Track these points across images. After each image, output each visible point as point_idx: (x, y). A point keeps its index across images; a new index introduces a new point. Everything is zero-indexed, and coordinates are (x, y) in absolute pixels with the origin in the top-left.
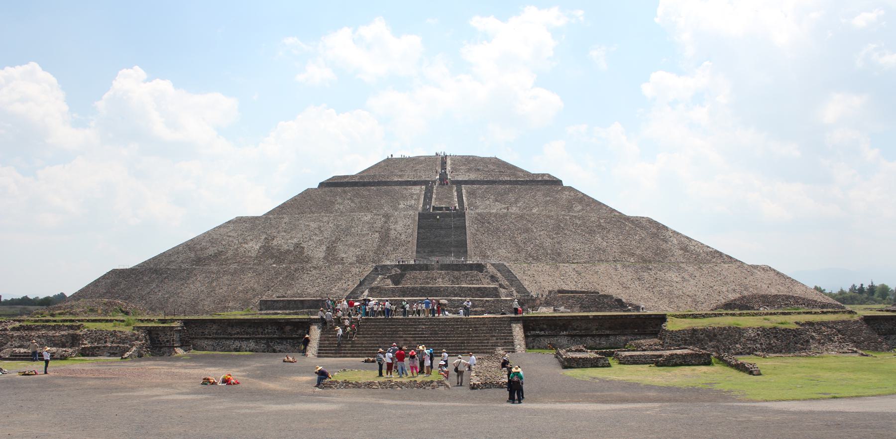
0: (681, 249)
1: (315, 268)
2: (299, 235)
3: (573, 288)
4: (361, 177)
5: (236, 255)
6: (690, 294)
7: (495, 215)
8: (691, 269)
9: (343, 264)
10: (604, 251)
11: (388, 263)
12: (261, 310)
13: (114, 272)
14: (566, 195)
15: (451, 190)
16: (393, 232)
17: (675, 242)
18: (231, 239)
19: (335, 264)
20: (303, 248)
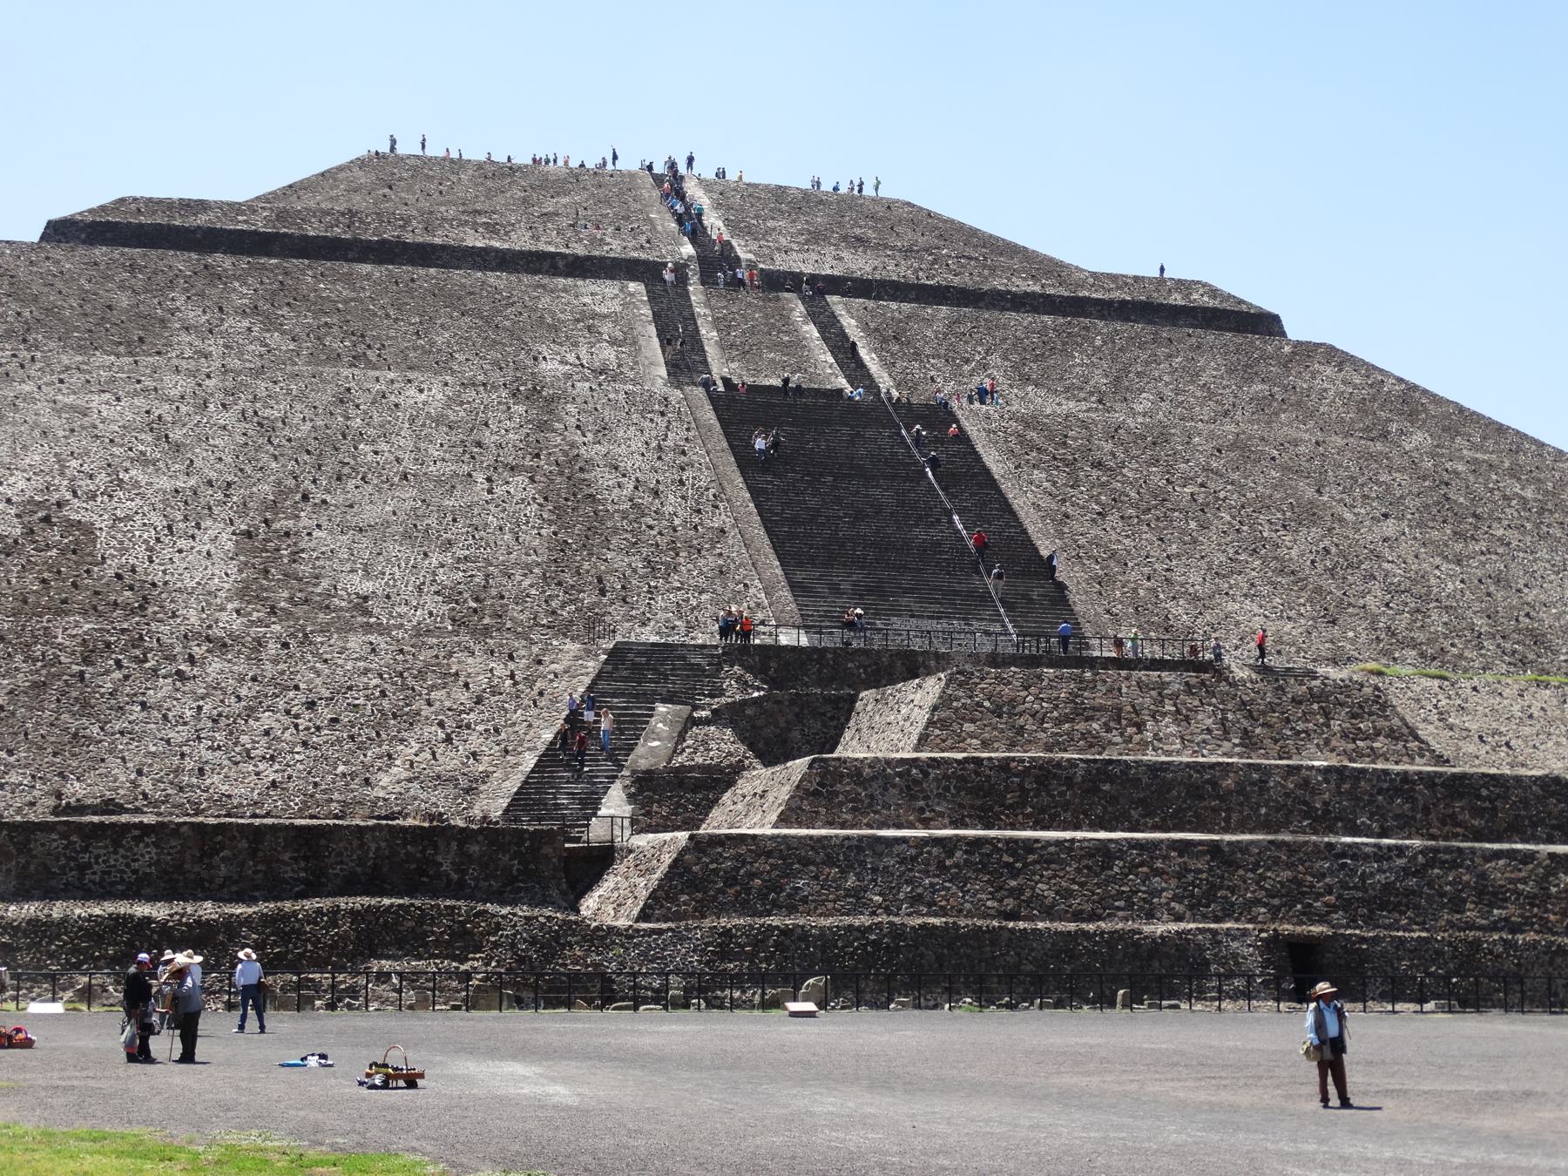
15: (786, 319)
16: (604, 479)
20: (88, 530)
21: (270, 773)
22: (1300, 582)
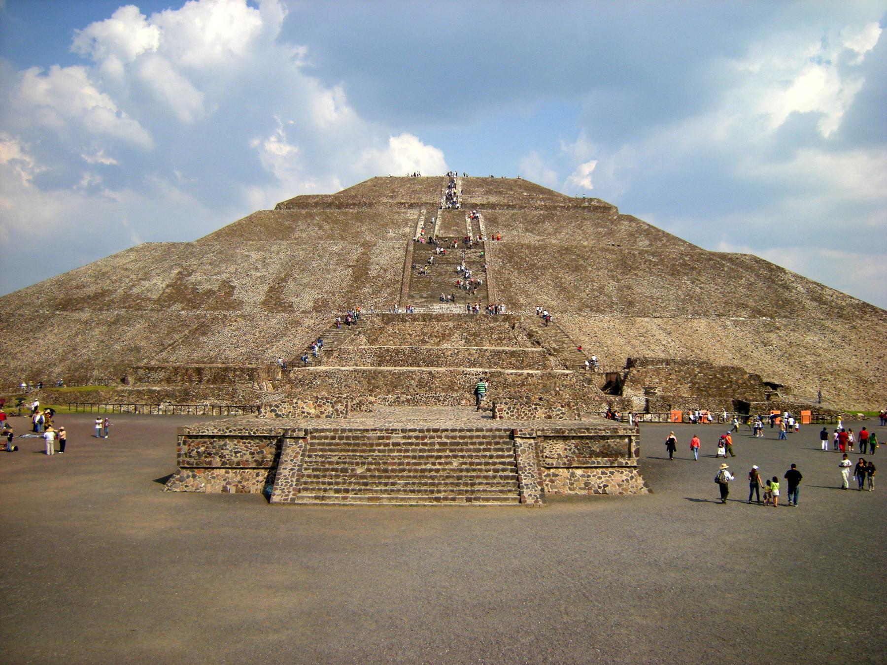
0: (813, 299)
1: (243, 317)
2: (232, 269)
3: (662, 356)
4: (338, 197)
5: (127, 297)
7: (529, 247)
8: (838, 328)
10: (699, 301)
17: (800, 288)
18: (126, 273)
19: (279, 312)
20: (233, 288)
21: (244, 350)
22: (564, 289)
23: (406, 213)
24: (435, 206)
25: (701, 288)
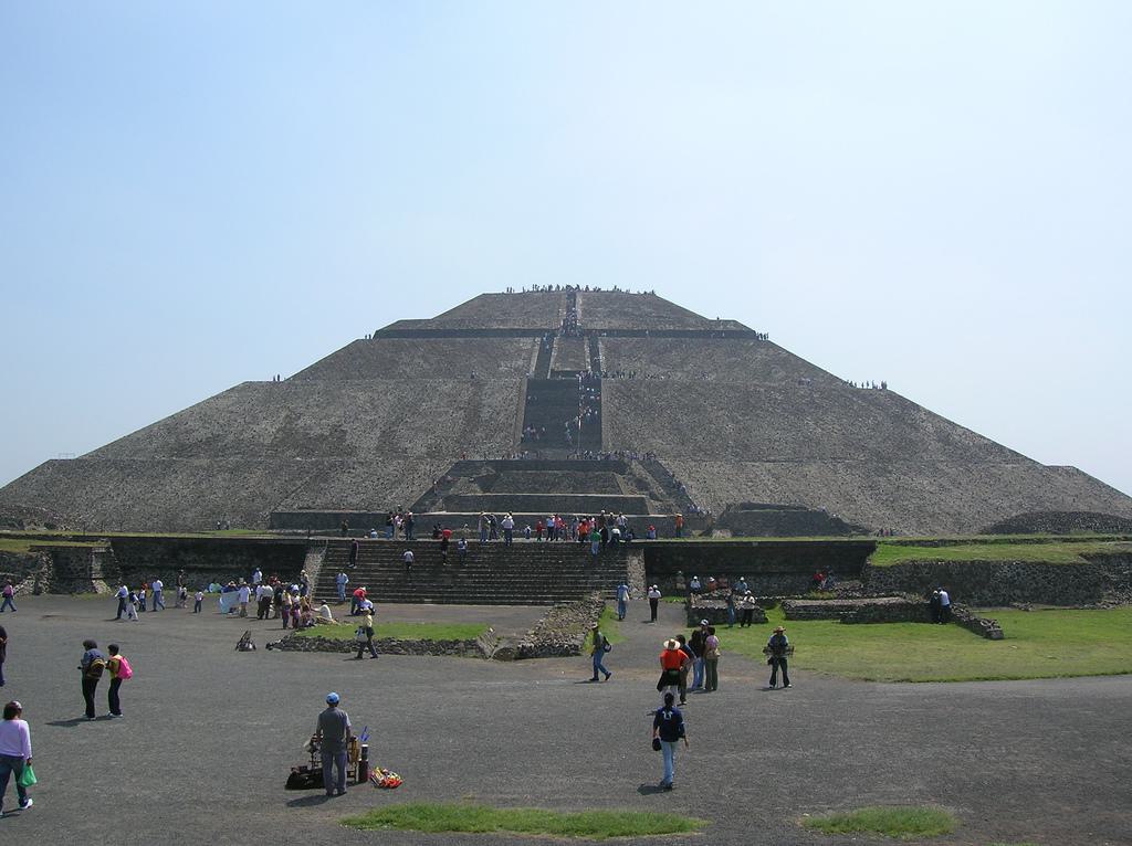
3: (767, 501)
6: (952, 512)
9: (406, 458)
11: (477, 458)
12: (272, 527)
13: (51, 463)
14: (761, 354)
16: (486, 409)
20: (345, 432)
23: (518, 342)
24: (553, 334)
25: (823, 429)
